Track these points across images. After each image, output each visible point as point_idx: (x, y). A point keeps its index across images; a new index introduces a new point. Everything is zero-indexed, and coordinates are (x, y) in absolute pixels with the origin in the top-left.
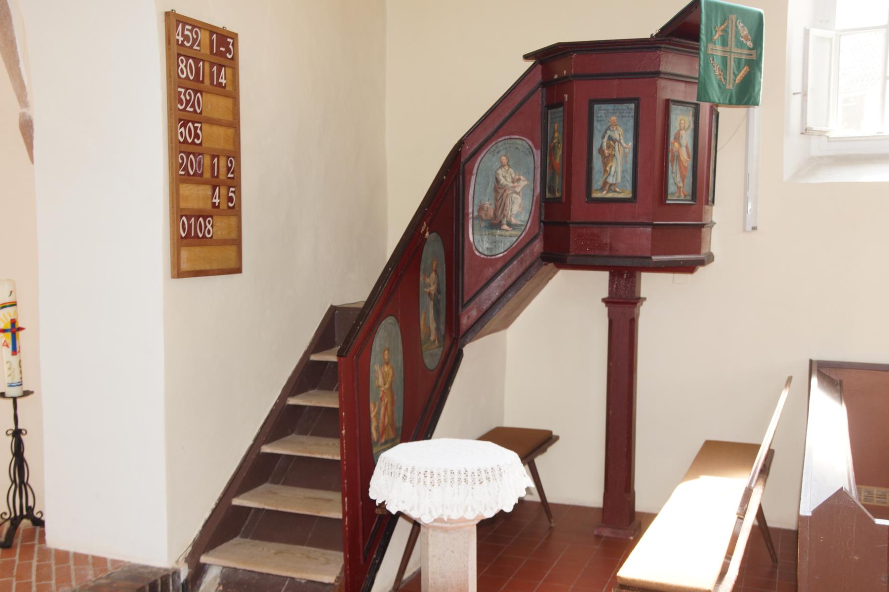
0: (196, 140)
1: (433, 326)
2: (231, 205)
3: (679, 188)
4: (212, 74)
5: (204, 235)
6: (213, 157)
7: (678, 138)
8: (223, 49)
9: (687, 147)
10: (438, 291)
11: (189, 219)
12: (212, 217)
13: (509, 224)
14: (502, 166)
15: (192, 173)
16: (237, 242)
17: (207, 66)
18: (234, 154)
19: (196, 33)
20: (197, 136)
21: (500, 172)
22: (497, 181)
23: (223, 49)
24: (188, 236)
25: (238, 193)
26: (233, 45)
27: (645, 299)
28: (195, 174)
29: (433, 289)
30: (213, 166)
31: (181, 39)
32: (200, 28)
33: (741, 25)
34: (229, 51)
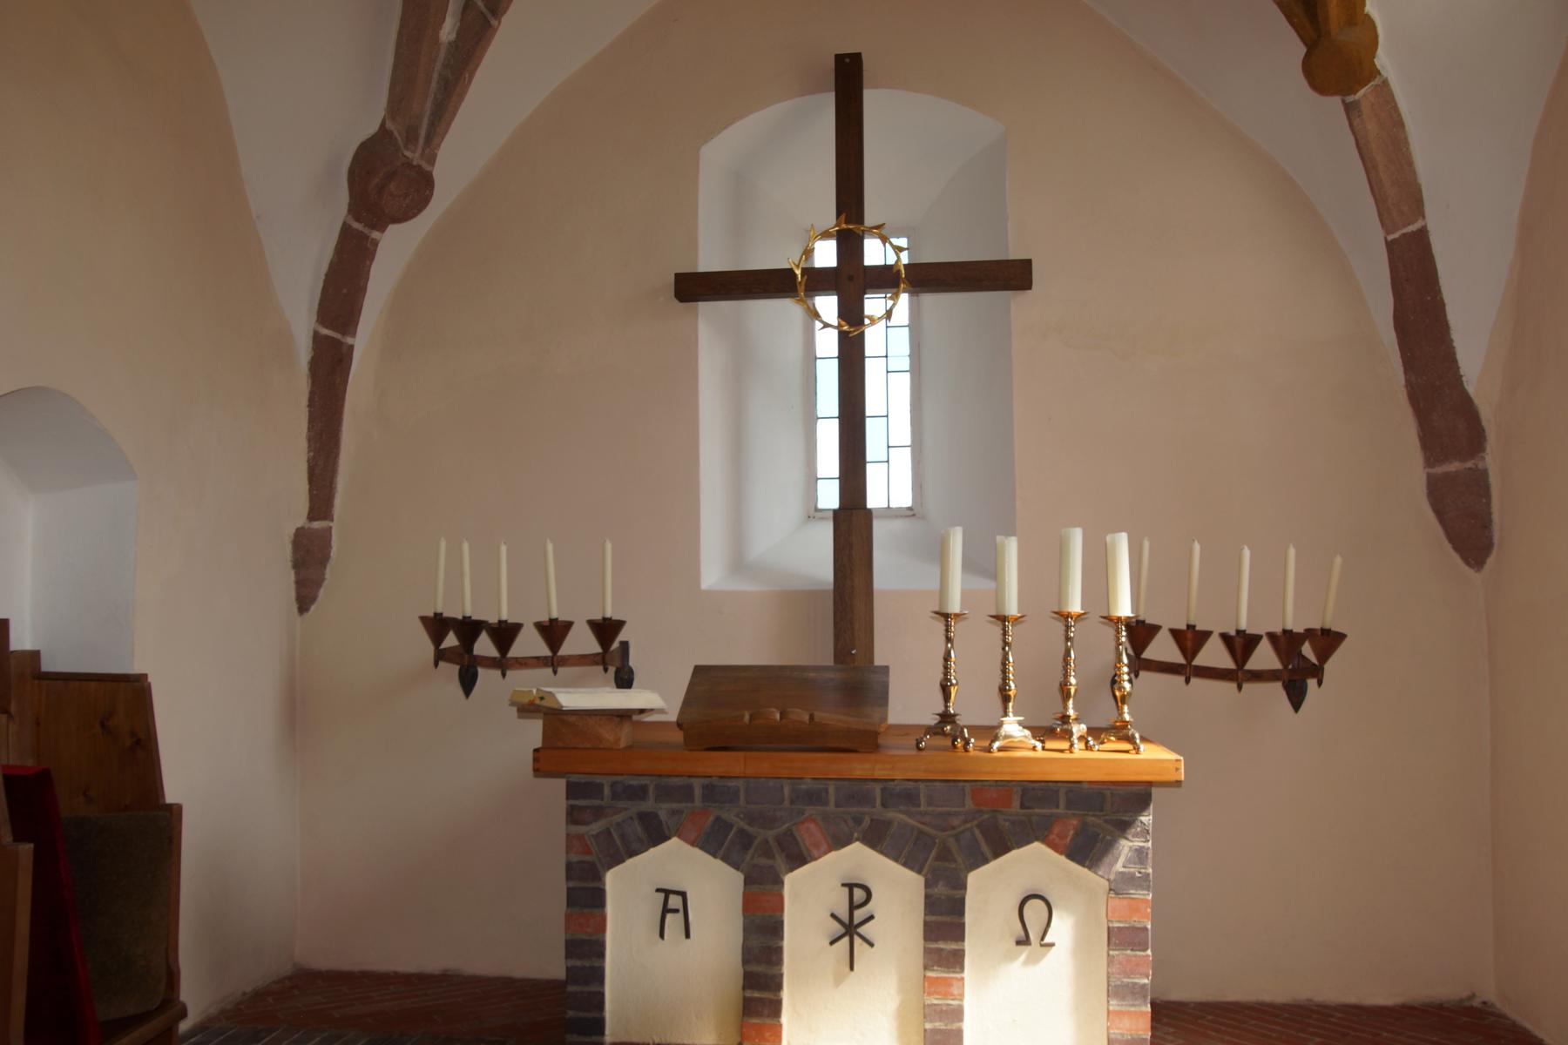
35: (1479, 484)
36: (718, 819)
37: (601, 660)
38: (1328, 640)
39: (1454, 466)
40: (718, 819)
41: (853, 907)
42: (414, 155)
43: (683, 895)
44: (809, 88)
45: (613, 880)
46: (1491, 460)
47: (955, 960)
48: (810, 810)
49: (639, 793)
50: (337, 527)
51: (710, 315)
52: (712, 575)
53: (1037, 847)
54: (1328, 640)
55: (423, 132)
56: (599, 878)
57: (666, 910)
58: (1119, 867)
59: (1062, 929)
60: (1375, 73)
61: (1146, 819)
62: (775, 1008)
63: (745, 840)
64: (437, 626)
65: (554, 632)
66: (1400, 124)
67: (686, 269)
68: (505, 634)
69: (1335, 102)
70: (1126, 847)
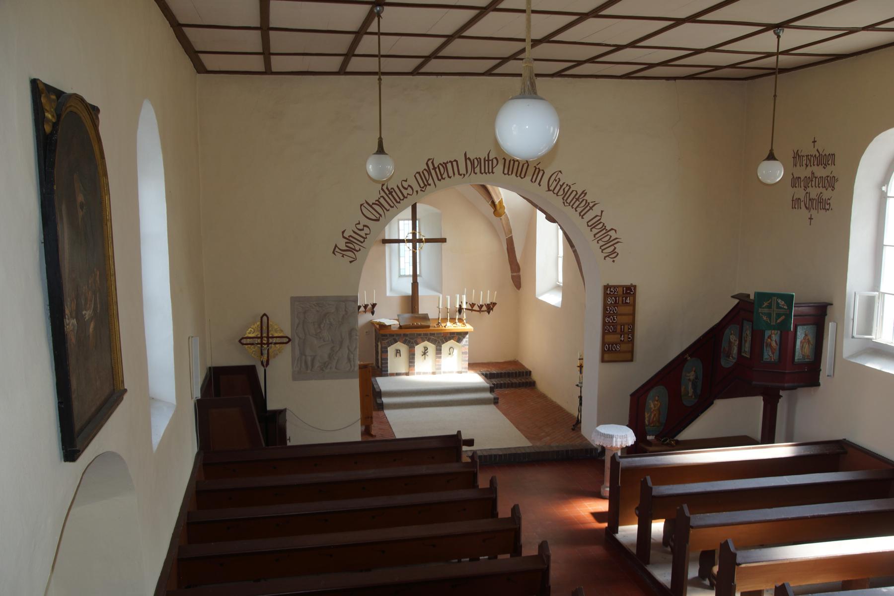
1: (691, 391)
2: (629, 340)
4: (623, 300)
7: (770, 337)
8: (628, 291)
9: (776, 341)
10: (696, 378)
13: (732, 357)
14: (731, 334)
15: (611, 331)
16: (632, 352)
17: (621, 299)
18: (633, 324)
19: (616, 289)
20: (614, 320)
21: (731, 336)
22: (730, 339)
23: (628, 291)
24: (609, 350)
25: (633, 336)
26: (634, 289)
27: (782, 396)
28: (613, 331)
29: (692, 378)
30: (621, 328)
31: (609, 292)
34: (632, 291)
35: (519, 277)
36: (405, 339)
38: (494, 304)
39: (515, 274)
40: (405, 339)
41: (425, 351)
45: (389, 349)
46: (521, 273)
47: (440, 357)
48: (419, 337)
49: (393, 335)
52: (388, 294)
53: (452, 340)
54: (494, 304)
56: (387, 348)
57: (397, 353)
58: (464, 343)
59: (456, 352)
60: (505, 213)
61: (467, 336)
62: (414, 366)
63: (409, 342)
66: (509, 220)
69: (498, 218)
70: (465, 340)
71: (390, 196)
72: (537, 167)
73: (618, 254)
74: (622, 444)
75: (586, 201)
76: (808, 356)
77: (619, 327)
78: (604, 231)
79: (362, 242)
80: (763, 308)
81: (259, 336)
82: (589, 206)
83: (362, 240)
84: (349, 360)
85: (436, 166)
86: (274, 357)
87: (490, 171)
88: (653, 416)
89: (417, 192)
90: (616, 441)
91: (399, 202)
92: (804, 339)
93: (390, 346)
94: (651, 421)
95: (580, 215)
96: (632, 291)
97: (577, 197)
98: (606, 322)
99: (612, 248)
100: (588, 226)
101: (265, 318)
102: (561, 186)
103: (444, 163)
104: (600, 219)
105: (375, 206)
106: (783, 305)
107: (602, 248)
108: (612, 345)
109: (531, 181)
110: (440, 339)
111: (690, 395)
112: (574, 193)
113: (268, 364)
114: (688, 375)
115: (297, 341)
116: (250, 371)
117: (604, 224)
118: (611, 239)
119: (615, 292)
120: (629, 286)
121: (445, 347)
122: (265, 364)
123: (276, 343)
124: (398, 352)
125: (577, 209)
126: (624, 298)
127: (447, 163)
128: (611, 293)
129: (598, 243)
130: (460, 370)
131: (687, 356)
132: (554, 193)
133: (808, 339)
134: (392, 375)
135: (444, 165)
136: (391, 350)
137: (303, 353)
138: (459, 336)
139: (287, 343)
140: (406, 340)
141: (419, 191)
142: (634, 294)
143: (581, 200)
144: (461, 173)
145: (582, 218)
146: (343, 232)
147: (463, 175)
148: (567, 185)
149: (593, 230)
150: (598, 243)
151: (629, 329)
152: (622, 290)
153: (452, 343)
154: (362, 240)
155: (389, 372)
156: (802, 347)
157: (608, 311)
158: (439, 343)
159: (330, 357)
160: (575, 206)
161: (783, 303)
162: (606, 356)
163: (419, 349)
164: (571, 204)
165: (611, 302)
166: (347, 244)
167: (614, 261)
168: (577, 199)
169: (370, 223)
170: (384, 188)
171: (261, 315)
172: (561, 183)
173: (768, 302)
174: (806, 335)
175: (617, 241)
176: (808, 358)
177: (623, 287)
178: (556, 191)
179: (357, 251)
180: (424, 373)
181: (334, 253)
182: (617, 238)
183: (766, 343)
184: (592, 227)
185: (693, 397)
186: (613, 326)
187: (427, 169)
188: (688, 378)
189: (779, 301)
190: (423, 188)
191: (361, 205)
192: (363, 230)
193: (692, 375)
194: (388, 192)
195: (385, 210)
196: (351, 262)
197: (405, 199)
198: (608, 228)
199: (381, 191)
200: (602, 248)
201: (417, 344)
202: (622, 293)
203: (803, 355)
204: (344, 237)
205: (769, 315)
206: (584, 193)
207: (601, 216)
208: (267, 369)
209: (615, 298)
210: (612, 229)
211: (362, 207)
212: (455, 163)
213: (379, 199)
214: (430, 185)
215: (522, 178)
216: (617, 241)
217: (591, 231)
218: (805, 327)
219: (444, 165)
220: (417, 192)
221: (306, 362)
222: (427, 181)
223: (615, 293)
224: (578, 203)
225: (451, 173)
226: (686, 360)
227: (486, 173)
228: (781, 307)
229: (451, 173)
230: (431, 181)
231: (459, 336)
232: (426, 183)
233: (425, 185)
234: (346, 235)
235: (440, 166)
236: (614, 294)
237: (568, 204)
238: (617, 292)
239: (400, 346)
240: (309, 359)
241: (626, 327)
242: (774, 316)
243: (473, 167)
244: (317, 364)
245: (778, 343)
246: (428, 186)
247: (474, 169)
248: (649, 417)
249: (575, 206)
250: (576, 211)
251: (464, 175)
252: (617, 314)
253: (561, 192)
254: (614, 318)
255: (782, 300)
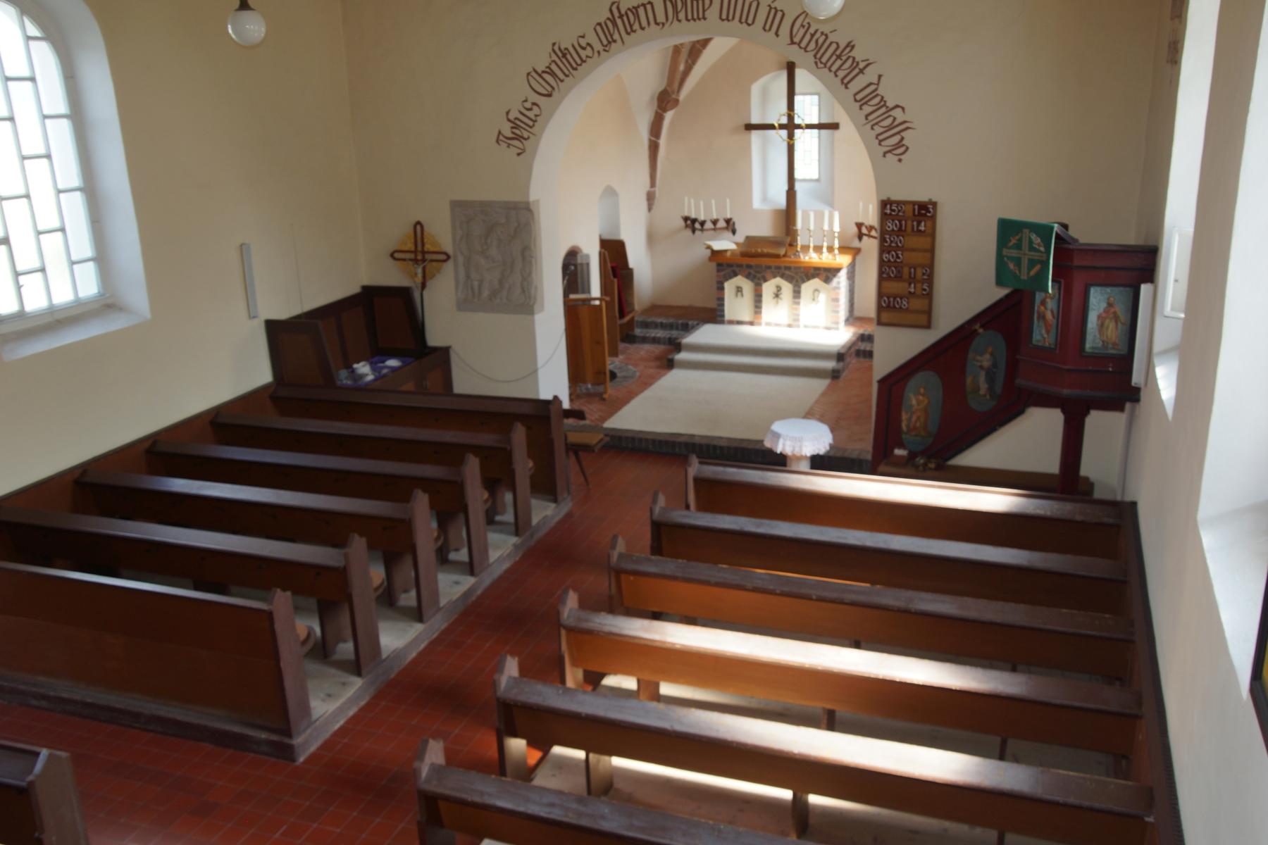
0: (898, 260)
1: (983, 387)
2: (924, 293)
3: (1044, 338)
5: (901, 308)
6: (910, 268)
8: (923, 212)
9: (1052, 312)
10: (995, 365)
11: (888, 298)
12: (908, 299)
15: (892, 275)
16: (929, 312)
17: (909, 223)
18: (931, 266)
19: (901, 207)
20: (898, 257)
23: (923, 212)
24: (888, 306)
26: (933, 209)
28: (896, 277)
29: (986, 364)
30: (910, 273)
31: (888, 211)
32: (904, 204)
33: (1034, 235)
34: (930, 212)
37: (727, 228)
41: (778, 291)
42: (674, 96)
43: (741, 288)
44: (780, 68)
45: (727, 285)
48: (769, 271)
50: (657, 189)
51: (755, 136)
52: (757, 204)
55: (676, 90)
59: (822, 297)
62: (760, 313)
64: (686, 219)
65: (715, 222)
67: (747, 122)
68: (703, 223)
71: (564, 60)
72: (773, 6)
73: (907, 148)
74: (794, 450)
75: (854, 58)
76: (1114, 344)
77: (906, 270)
78: (884, 110)
79: (531, 127)
80: (1010, 248)
81: (413, 249)
82: (858, 68)
83: (531, 123)
84: (523, 291)
85: (623, 12)
86: (431, 278)
87: (701, 16)
88: (914, 418)
89: (599, 52)
90: (784, 445)
91: (576, 69)
92: (1106, 311)
93: (727, 280)
94: (911, 426)
95: (842, 83)
96: (930, 212)
97: (838, 53)
98: (884, 261)
99: (897, 138)
100: (856, 100)
101: (418, 227)
102: (812, 36)
103: (634, 7)
104: (876, 90)
105: (545, 76)
106: (1039, 245)
107: (881, 137)
108: (895, 298)
109: (764, 29)
110: (800, 275)
111: (982, 392)
112: (834, 46)
113: (424, 286)
114: (979, 358)
115: (461, 259)
116: (403, 294)
117: (882, 97)
118: (896, 123)
119: (899, 211)
120: (925, 202)
121: (807, 287)
122: (420, 286)
123: (432, 261)
124: (739, 290)
125: (838, 73)
126: (915, 223)
127: (638, 6)
128: (893, 213)
129: (872, 129)
130: (829, 325)
131: (977, 326)
132: (801, 48)
133: (1115, 313)
134: (731, 322)
135: (634, 10)
136: (729, 286)
137: (468, 276)
138: (828, 274)
139: (445, 261)
140: (750, 274)
141: (602, 53)
142: (933, 218)
143: (844, 58)
144: (658, 21)
145: (846, 88)
146: (508, 113)
147: (661, 26)
148: (822, 33)
149: (865, 107)
150: (872, 129)
151: (924, 274)
152: (911, 210)
153: (816, 282)
154: (531, 123)
155: (728, 316)
156: (1101, 326)
157: (887, 242)
158: (797, 281)
159: (501, 282)
160: (834, 68)
161: (1039, 240)
162: (886, 316)
163: (768, 288)
164: (828, 65)
165: (893, 230)
166: (514, 130)
167: (900, 160)
168: (839, 57)
169: (542, 101)
170: (556, 48)
171: (414, 222)
172: (812, 30)
173: (1017, 237)
174: (1110, 305)
175: (905, 126)
176: (1114, 348)
177: (914, 203)
178: (803, 45)
179: (525, 139)
180: (777, 325)
181: (498, 141)
182: (905, 122)
183: (1038, 312)
184: (863, 103)
185: (988, 397)
186: (895, 268)
187: (611, 17)
188: (979, 364)
189: (1033, 236)
190: (606, 46)
191: (528, 74)
192: (530, 109)
193: (986, 361)
194: (560, 55)
195: (558, 81)
196: (519, 154)
197: (584, 64)
198: (890, 104)
199: (553, 55)
200: (881, 137)
201: (766, 280)
202: (911, 214)
203: (1103, 342)
204: (509, 120)
205: (1018, 262)
206: (851, 46)
207: (878, 84)
208: (425, 293)
209: (900, 221)
210: (897, 106)
211: (530, 77)
212: (649, 7)
213: (550, 64)
214: (615, 41)
215: (749, 25)
216: (905, 126)
217: (861, 109)
218: (1108, 290)
219: (634, 10)
220: (599, 52)
221: (472, 288)
222: (611, 36)
223: (900, 214)
224: (839, 63)
225: (644, 23)
226: (975, 333)
227: (694, 20)
228: (1035, 248)
229: (644, 23)
230: (616, 36)
231: (828, 274)
232: (610, 40)
233: (609, 43)
234: (511, 117)
235: (629, 13)
236: (897, 215)
237: (822, 66)
238: (904, 212)
239: (740, 280)
240: (476, 284)
241: (919, 272)
242: (1025, 262)
243: (676, 12)
244: (486, 293)
245: (1055, 312)
246: (613, 44)
247: (677, 13)
248: (909, 420)
249: (834, 68)
250: (836, 76)
251: (663, 24)
252: (903, 249)
253: (812, 45)
254: (897, 255)
255: (1038, 235)
